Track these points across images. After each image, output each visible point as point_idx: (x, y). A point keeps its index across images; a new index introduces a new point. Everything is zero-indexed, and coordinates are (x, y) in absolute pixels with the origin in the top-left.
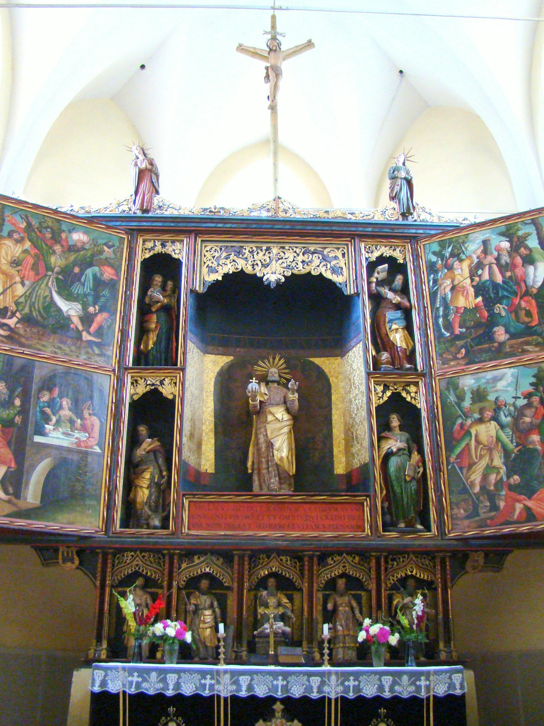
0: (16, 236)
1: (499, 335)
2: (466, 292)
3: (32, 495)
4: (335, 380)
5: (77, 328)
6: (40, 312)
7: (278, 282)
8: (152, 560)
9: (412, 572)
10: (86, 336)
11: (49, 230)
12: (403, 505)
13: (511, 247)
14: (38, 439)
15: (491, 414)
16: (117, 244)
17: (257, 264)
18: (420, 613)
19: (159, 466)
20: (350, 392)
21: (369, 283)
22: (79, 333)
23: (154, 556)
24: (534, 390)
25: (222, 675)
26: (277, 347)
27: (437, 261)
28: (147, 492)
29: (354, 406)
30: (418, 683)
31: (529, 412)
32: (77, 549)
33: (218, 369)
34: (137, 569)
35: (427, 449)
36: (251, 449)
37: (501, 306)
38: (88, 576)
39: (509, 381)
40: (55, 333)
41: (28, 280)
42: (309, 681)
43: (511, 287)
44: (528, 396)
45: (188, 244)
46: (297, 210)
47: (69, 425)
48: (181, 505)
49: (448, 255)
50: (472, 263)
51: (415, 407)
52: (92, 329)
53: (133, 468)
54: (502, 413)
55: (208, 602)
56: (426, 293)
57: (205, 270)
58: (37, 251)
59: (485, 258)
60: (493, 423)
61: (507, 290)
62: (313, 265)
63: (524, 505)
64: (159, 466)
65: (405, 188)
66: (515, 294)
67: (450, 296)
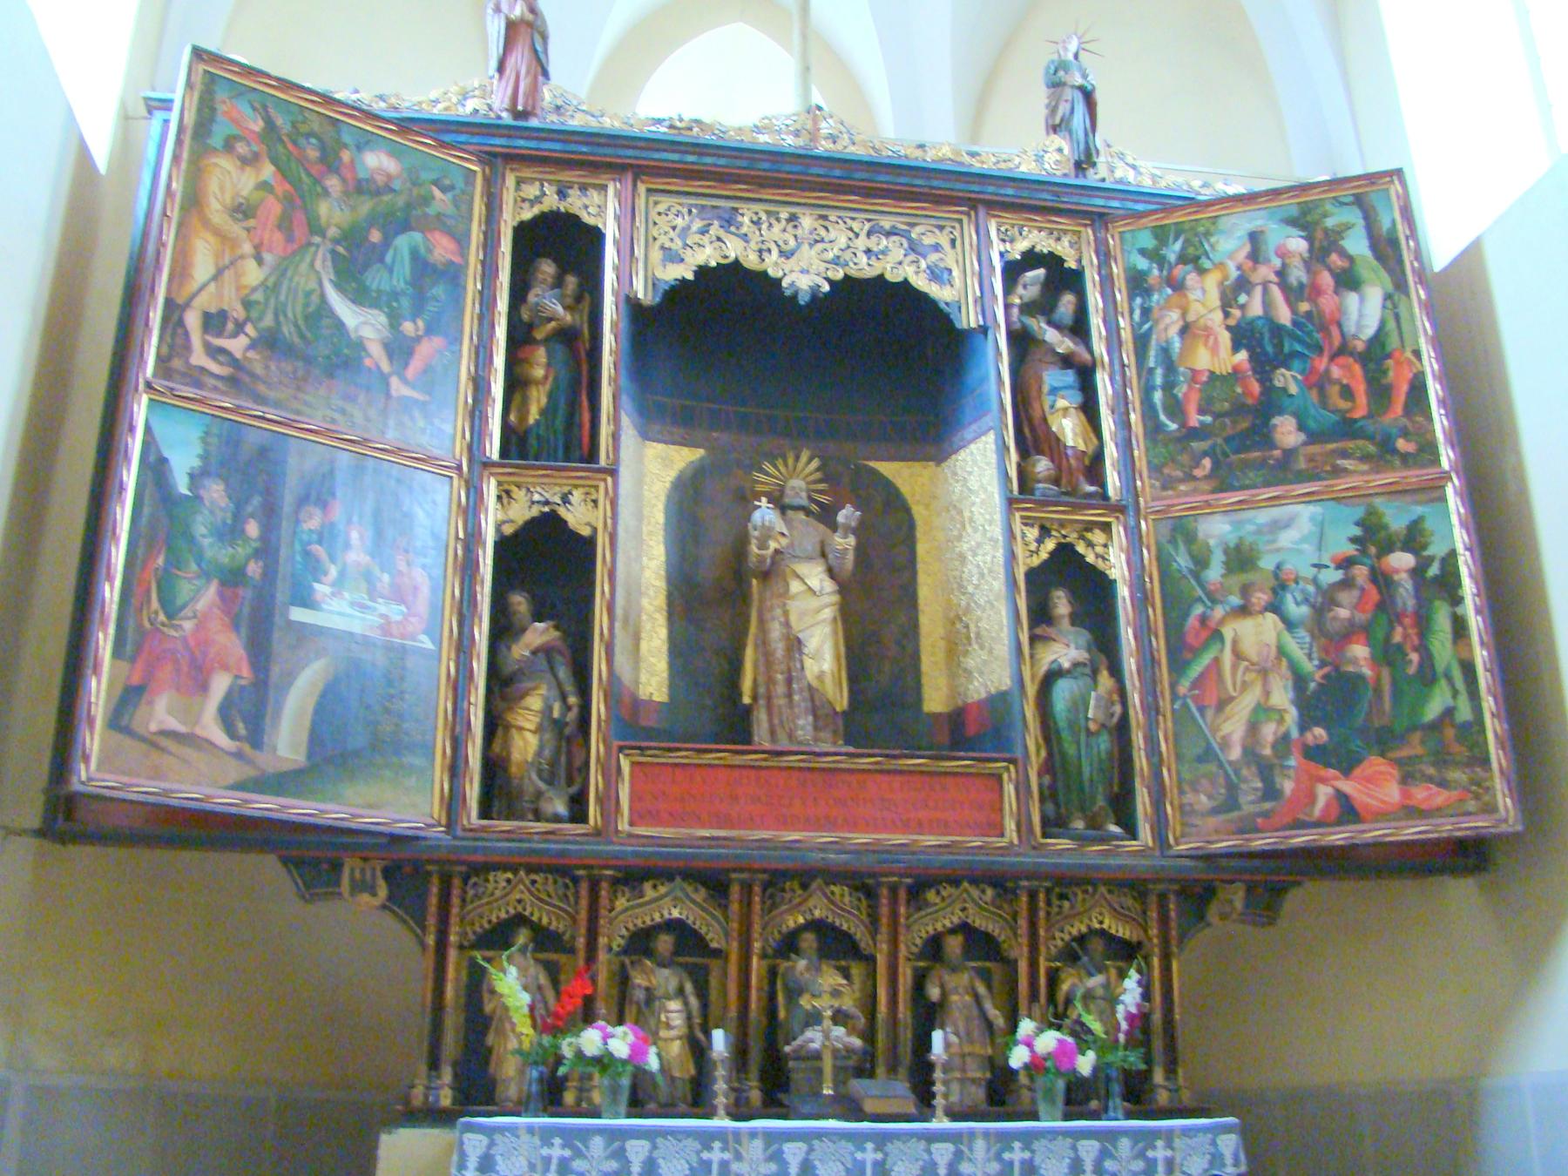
0: (241, 148)
2: (1211, 339)
3: (288, 741)
4: (924, 512)
5: (378, 367)
6: (296, 326)
7: (815, 290)
8: (551, 889)
9: (1101, 923)
10: (397, 387)
11: (313, 141)
12: (1081, 782)
13: (1311, 250)
14: (298, 614)
15: (1265, 597)
16: (460, 184)
17: (769, 251)
18: (1133, 1010)
19: (559, 685)
20: (959, 538)
21: (1007, 307)
22: (385, 379)
23: (555, 882)
25: (745, 1140)
26: (797, 433)
27: (1150, 269)
28: (533, 740)
29: (970, 567)
30: (1150, 1154)
31: (1346, 597)
32: (384, 863)
33: (670, 475)
34: (520, 909)
35: (1130, 664)
36: (749, 654)
37: (1288, 373)
38: (405, 922)
39: (1306, 532)
40: (331, 376)
41: (270, 250)
42: (929, 1152)
43: (1311, 337)
44: (1345, 563)
45: (618, 194)
46: (857, 139)
47: (364, 585)
48: (614, 770)
49: (1172, 257)
50: (1226, 278)
51: (1103, 575)
52: (410, 373)
53: (503, 685)
54: (1289, 598)
55: (673, 984)
56: (1126, 335)
57: (656, 255)
58: (288, 187)
59: (1254, 269)
60: (1271, 617)
61: (1299, 341)
62: (889, 258)
63: (1338, 791)
64: (559, 685)
65: (1080, 108)
66: (1319, 350)
67: (1177, 345)
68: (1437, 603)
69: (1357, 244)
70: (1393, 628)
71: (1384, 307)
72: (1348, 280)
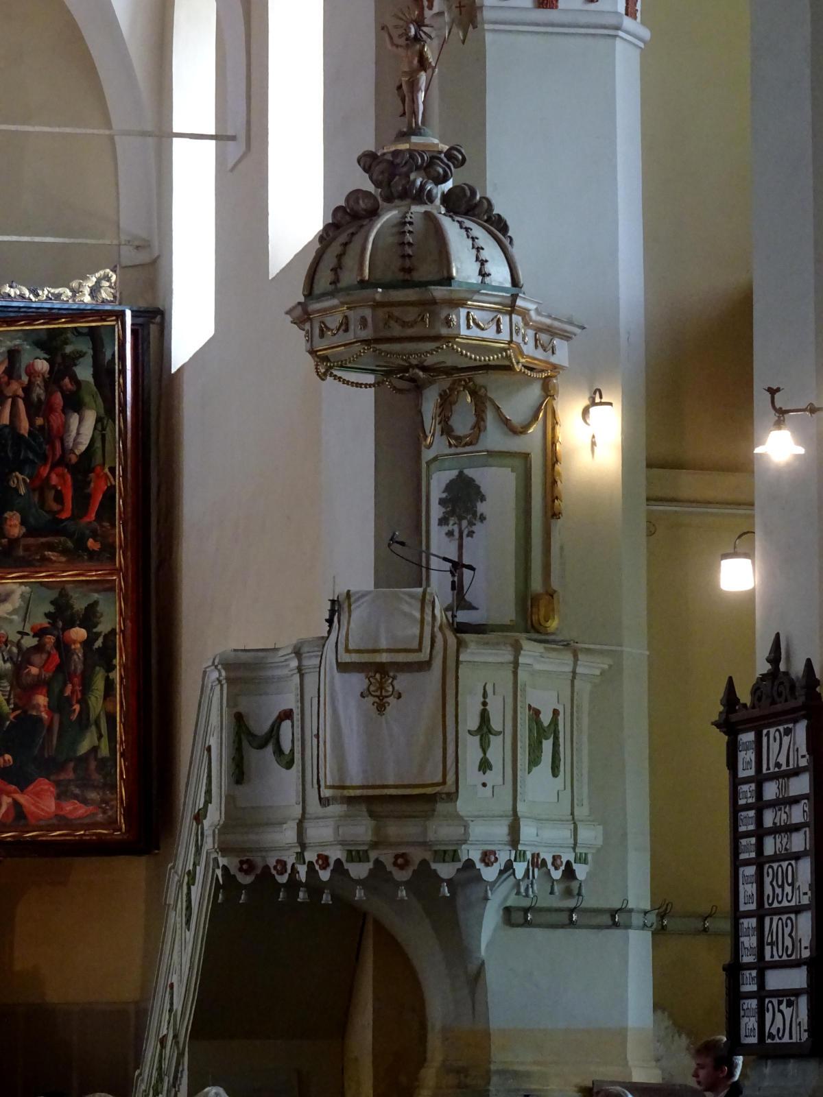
1: (11, 526)
13: (51, 372)
24: (48, 625)
31: (38, 659)
37: (20, 477)
39: (17, 605)
44: (40, 633)
59: (8, 384)
66: (44, 458)
68: (98, 668)
69: (84, 372)
70: (65, 685)
71: (95, 428)
72: (74, 404)
